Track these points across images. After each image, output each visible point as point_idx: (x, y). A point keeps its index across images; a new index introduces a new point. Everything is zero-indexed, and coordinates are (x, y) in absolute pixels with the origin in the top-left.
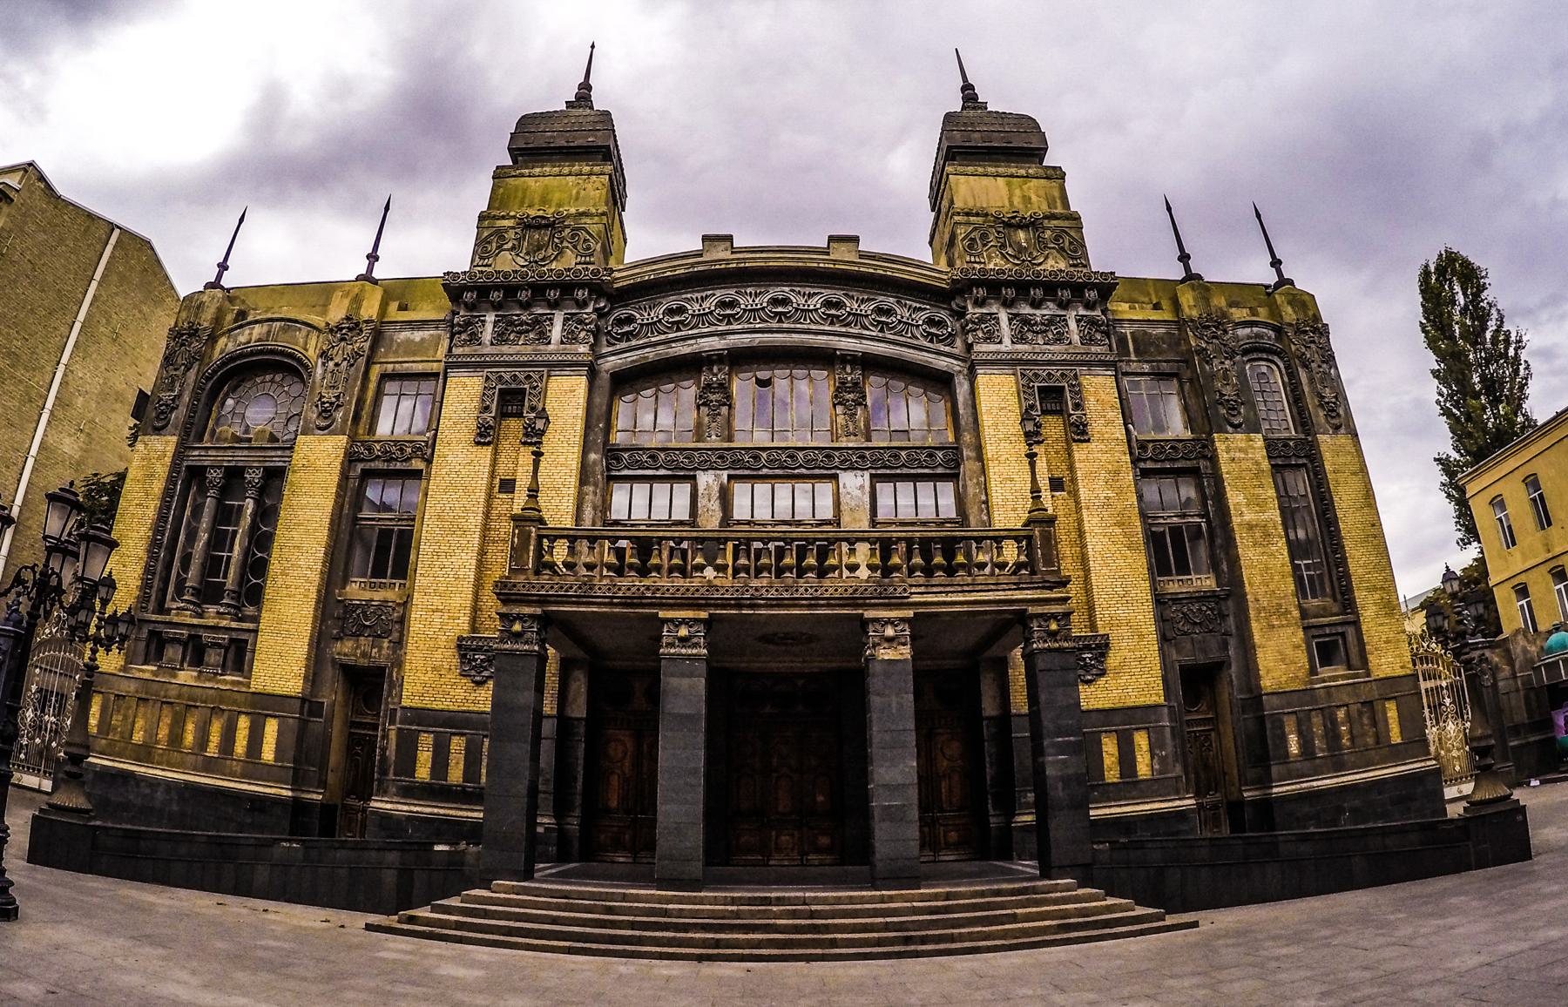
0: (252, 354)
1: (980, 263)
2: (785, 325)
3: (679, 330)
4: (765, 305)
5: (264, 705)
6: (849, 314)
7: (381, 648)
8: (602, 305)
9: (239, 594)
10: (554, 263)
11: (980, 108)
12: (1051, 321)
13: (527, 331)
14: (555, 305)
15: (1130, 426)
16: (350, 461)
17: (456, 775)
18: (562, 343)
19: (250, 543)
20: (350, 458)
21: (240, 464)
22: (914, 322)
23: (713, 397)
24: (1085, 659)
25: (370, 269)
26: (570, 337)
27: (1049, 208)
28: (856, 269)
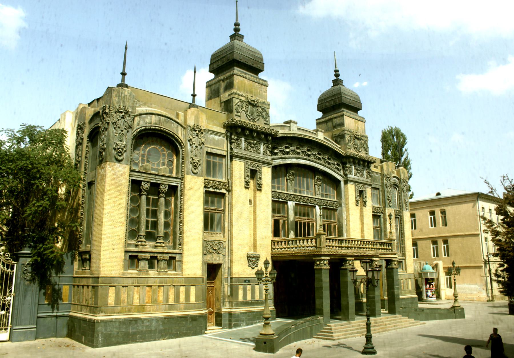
5: (191, 281)
14: (261, 140)
17: (249, 298)
21: (158, 182)
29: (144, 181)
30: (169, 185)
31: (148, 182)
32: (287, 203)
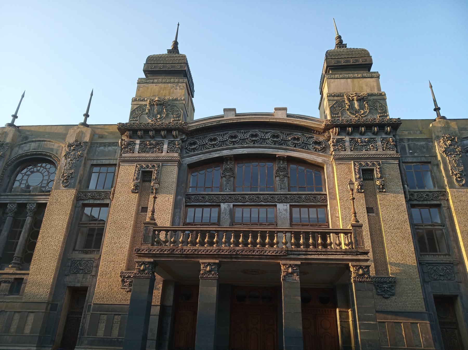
0: (31, 155)
1: (338, 117)
2: (256, 145)
3: (214, 147)
4: (248, 137)
6: (282, 140)
7: (87, 279)
8: (184, 137)
9: (21, 258)
10: (164, 120)
11: (343, 47)
12: (369, 141)
13: (153, 148)
14: (165, 137)
15: (406, 186)
16: (77, 200)
18: (168, 152)
19: (28, 236)
20: (78, 198)
21: (25, 202)
22: (309, 143)
23: (227, 174)
24: (384, 287)
25: (86, 120)
26: (170, 150)
27: (371, 91)
28: (285, 121)
29: (10, 203)
30: (37, 204)
31: (14, 203)
32: (220, 205)
